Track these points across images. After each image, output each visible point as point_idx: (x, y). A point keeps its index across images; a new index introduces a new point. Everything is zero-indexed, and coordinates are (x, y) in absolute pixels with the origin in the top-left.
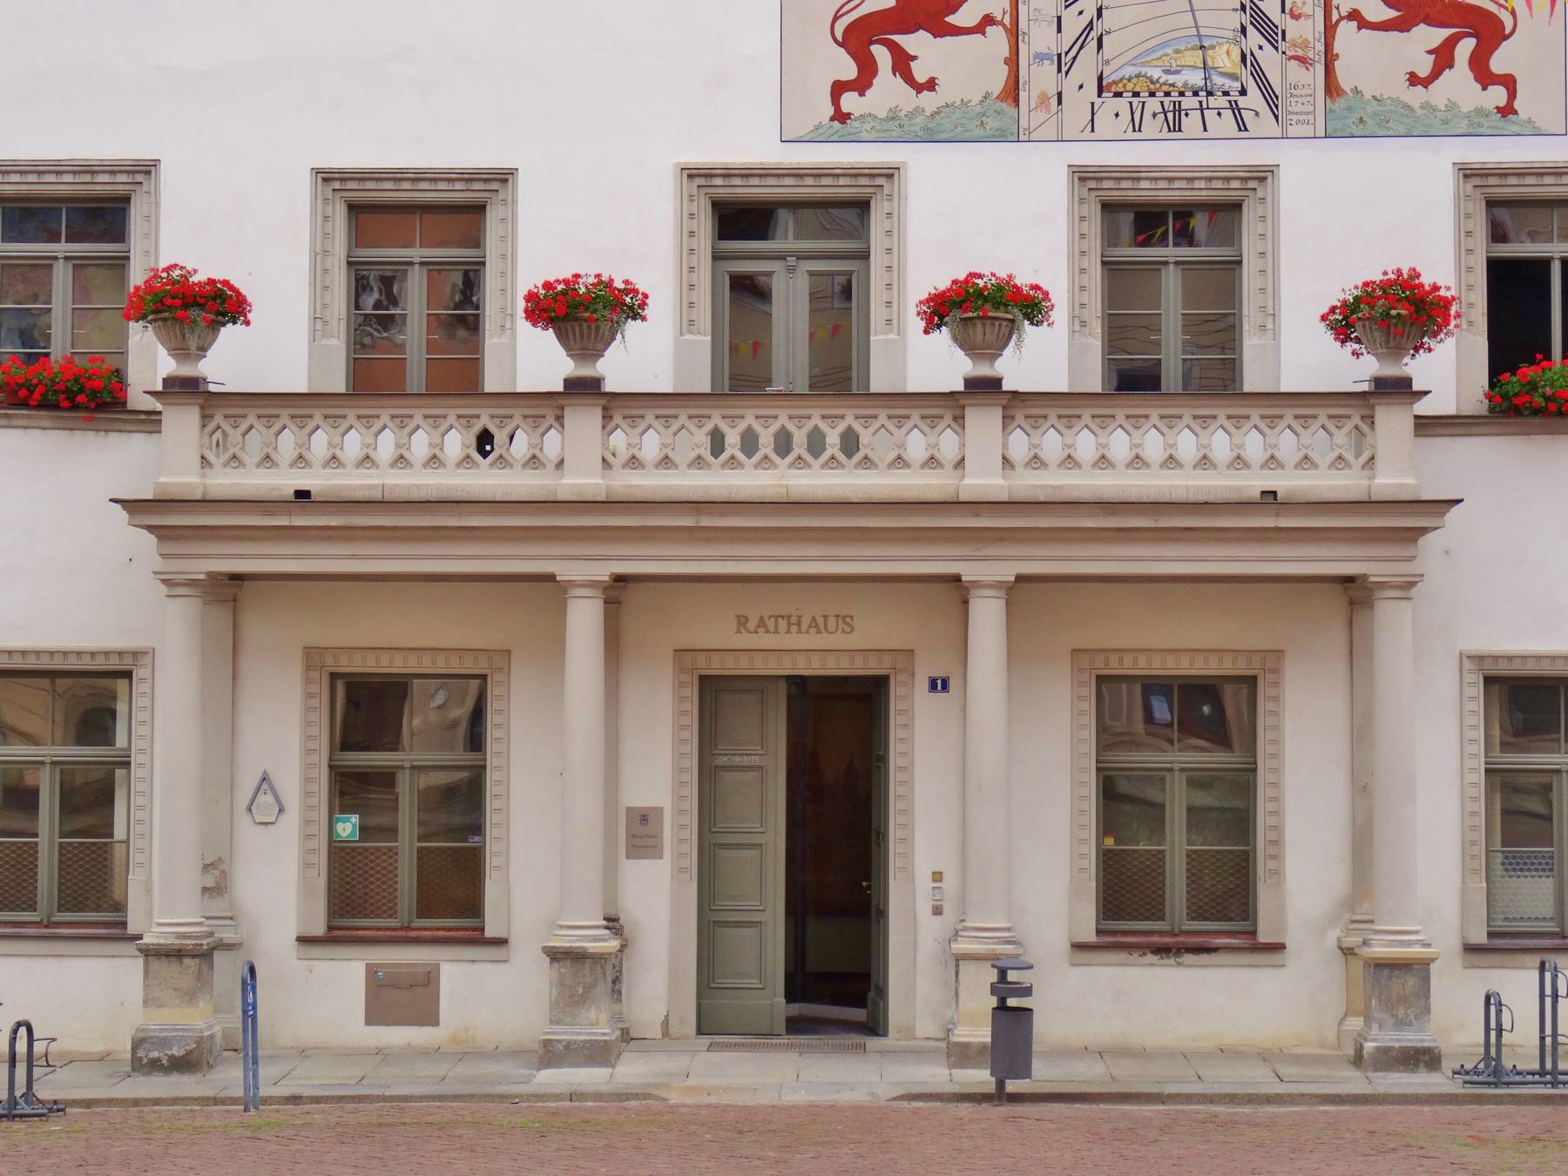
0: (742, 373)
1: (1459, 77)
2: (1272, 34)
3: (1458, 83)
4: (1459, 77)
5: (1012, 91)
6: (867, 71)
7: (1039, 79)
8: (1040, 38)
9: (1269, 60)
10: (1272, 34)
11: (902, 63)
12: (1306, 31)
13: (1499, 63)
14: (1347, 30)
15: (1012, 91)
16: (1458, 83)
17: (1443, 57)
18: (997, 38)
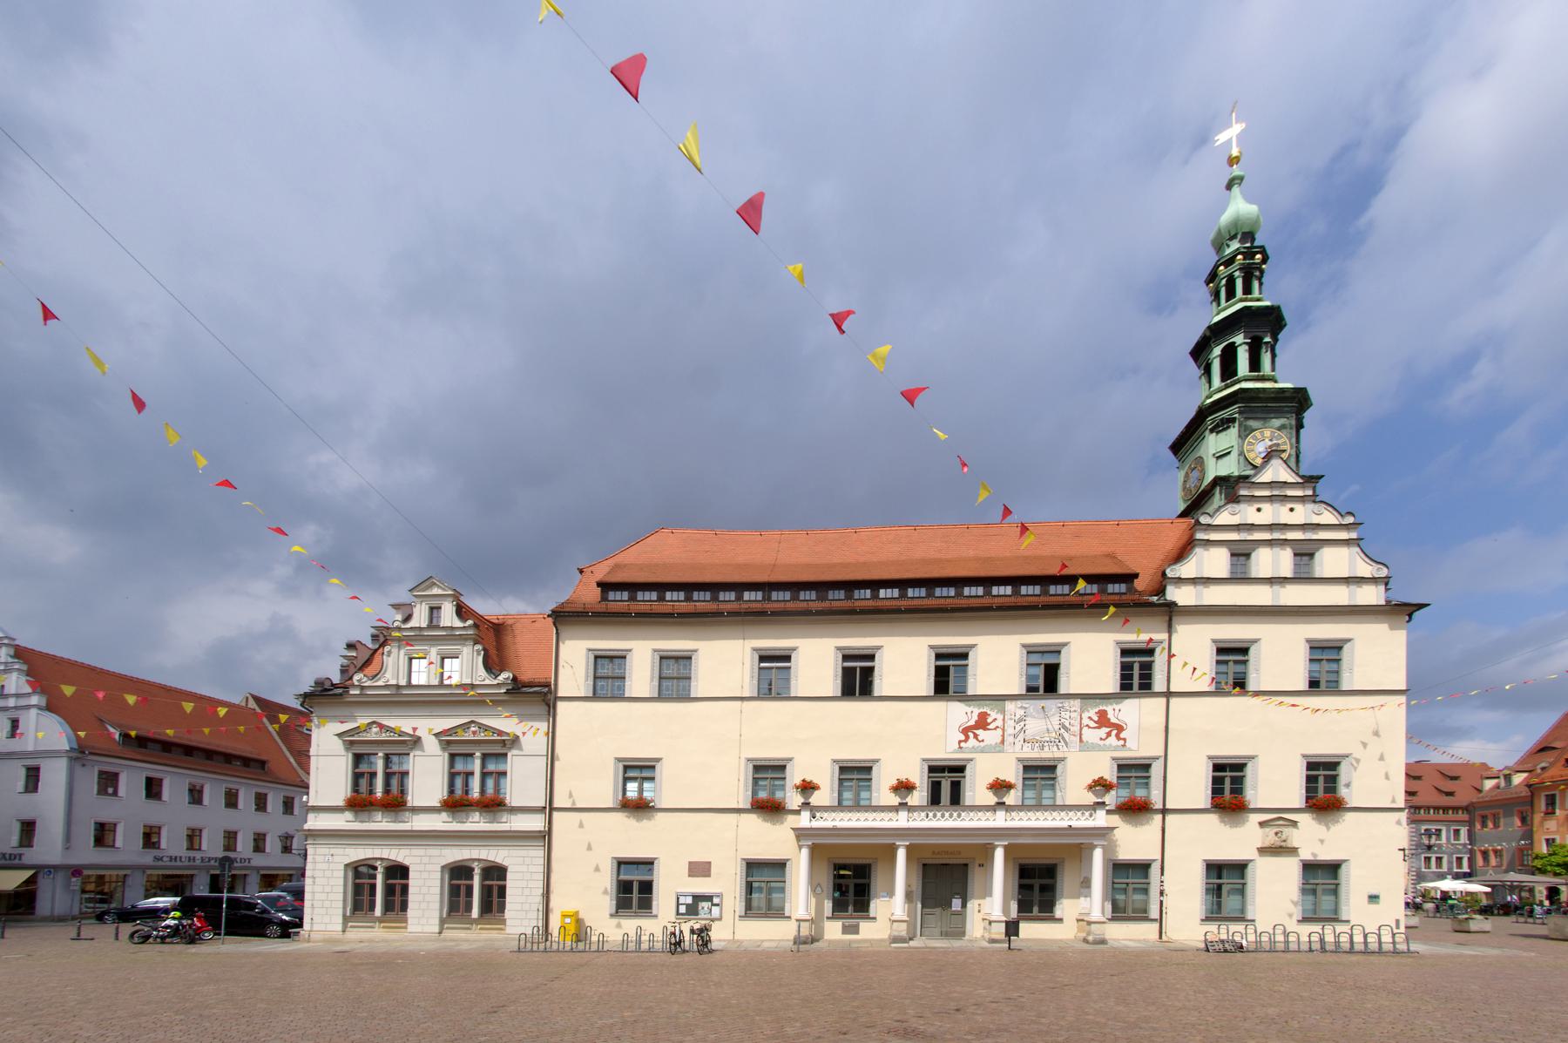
0: (935, 799)
1: (1113, 738)
2: (1067, 729)
3: (1112, 740)
4: (1113, 738)
5: (1003, 742)
6: (967, 738)
7: (1009, 740)
8: (1010, 731)
9: (1066, 735)
10: (1067, 729)
11: (976, 736)
12: (1077, 729)
13: (1123, 735)
14: (1085, 730)
15: (1003, 742)
16: (1112, 740)
17: (1109, 734)
18: (999, 732)
